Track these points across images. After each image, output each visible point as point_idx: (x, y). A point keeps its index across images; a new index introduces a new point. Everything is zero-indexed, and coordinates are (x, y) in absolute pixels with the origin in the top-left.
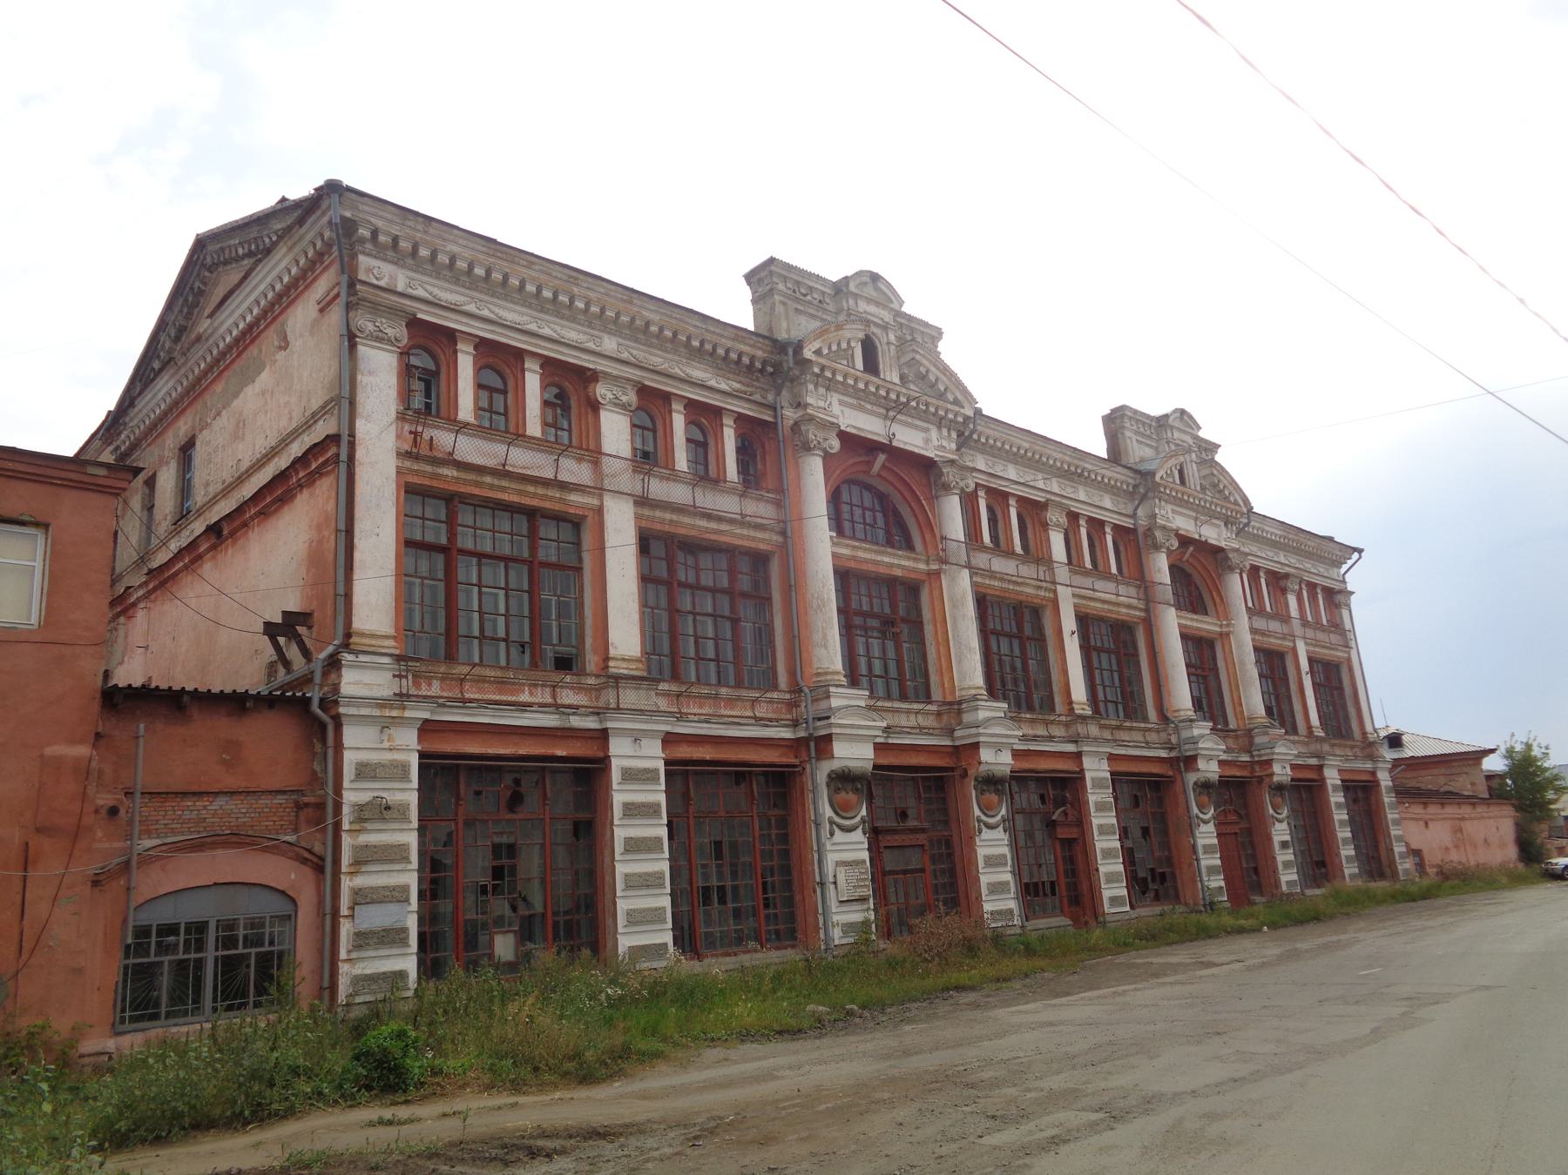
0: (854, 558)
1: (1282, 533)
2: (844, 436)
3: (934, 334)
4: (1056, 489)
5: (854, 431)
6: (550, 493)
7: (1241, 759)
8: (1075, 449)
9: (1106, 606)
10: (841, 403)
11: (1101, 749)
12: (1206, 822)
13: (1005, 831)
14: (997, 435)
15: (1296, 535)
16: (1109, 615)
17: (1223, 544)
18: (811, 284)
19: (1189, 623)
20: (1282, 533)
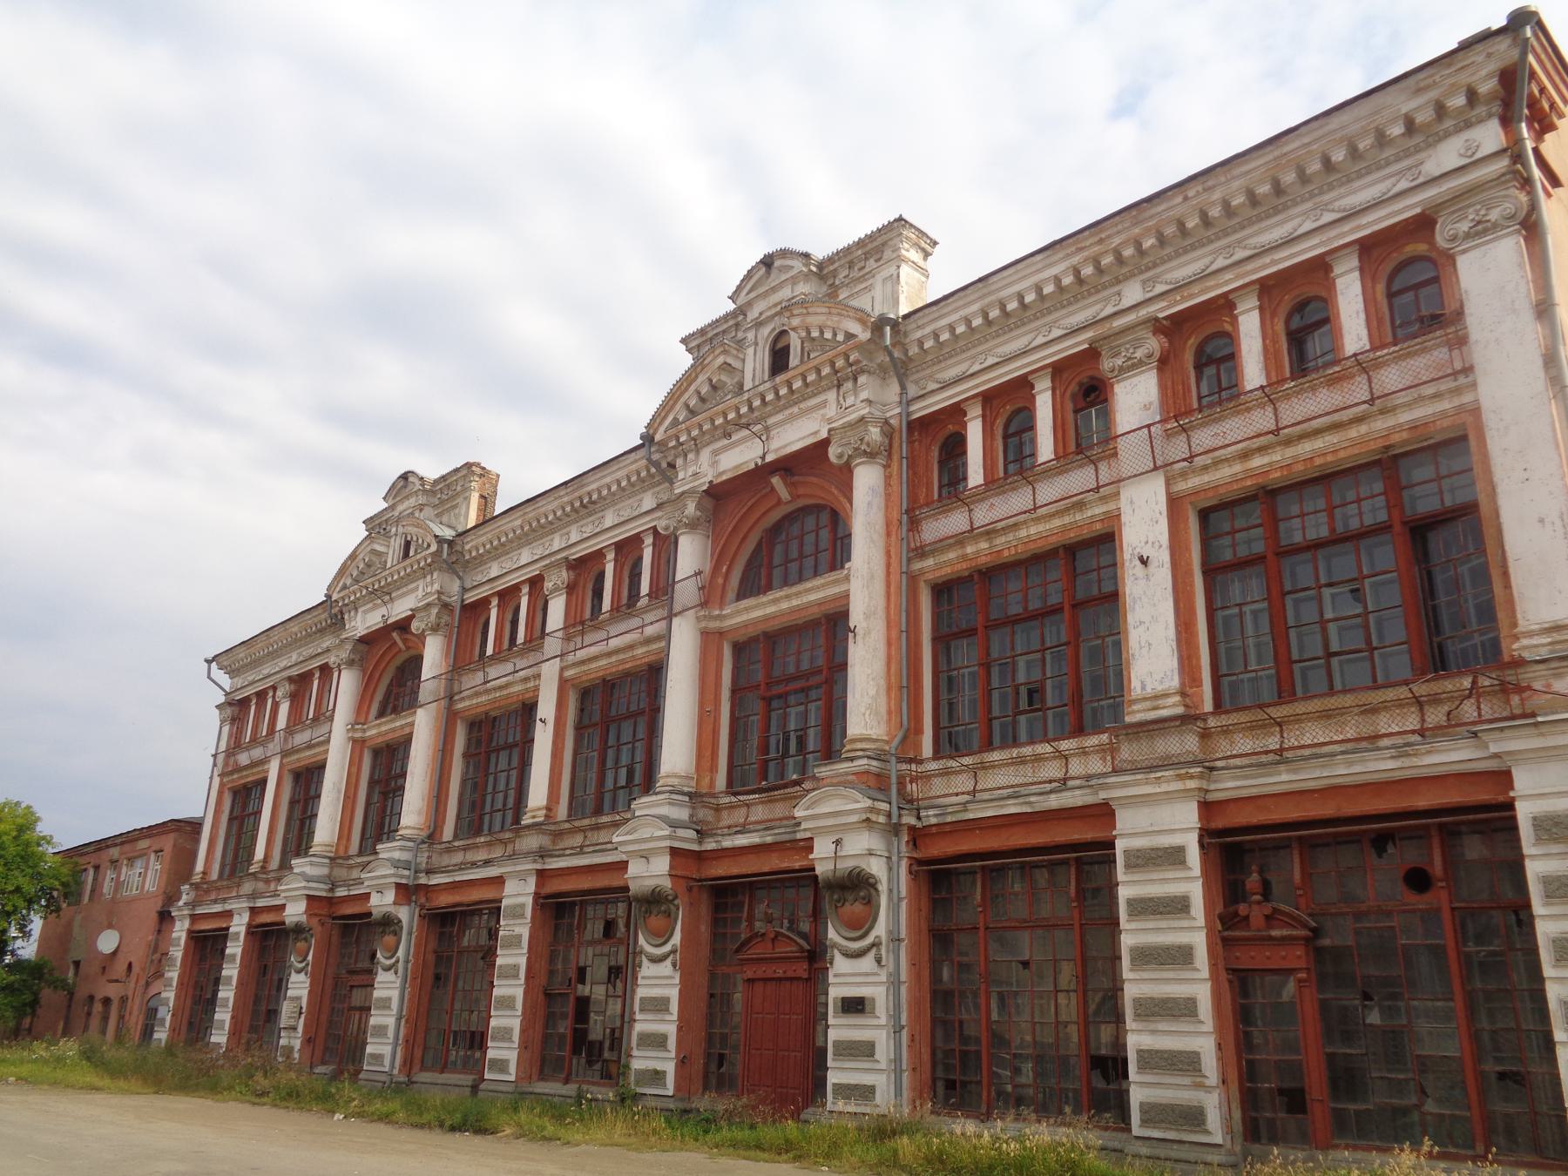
0: (380, 734)
1: (1075, 260)
2: (368, 640)
3: (464, 472)
4: (574, 538)
5: (365, 632)
6: (254, 770)
7: (799, 836)
8: (565, 483)
9: (614, 659)
10: (365, 612)
11: (519, 868)
12: (656, 960)
13: (396, 973)
14: (489, 536)
15: (1134, 225)
16: (621, 668)
17: (824, 434)
18: (384, 518)
19: (771, 609)
20: (1075, 260)
